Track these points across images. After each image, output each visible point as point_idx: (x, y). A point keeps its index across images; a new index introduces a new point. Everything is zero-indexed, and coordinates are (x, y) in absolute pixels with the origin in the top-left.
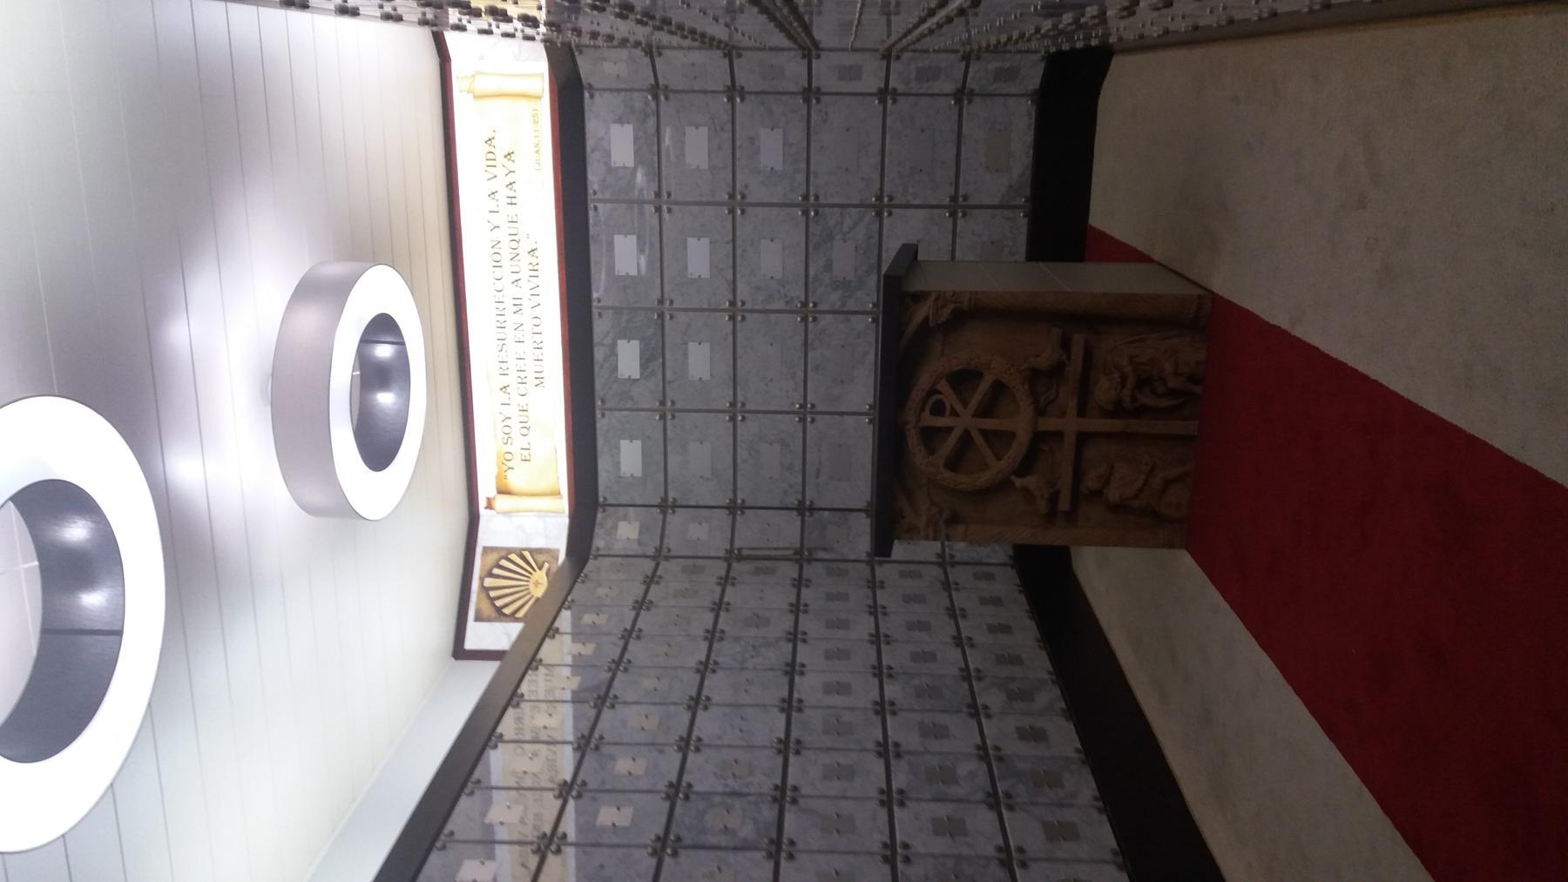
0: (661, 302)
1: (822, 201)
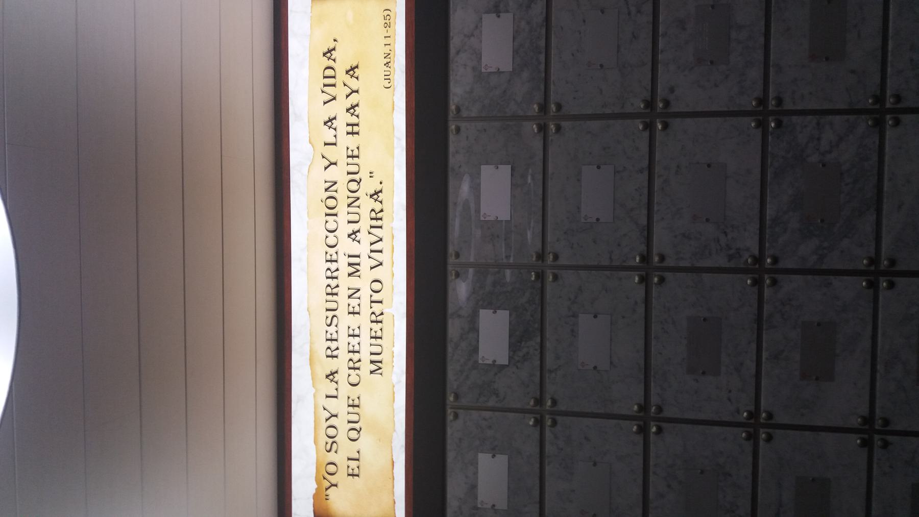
0: (541, 256)
1: (788, 105)
